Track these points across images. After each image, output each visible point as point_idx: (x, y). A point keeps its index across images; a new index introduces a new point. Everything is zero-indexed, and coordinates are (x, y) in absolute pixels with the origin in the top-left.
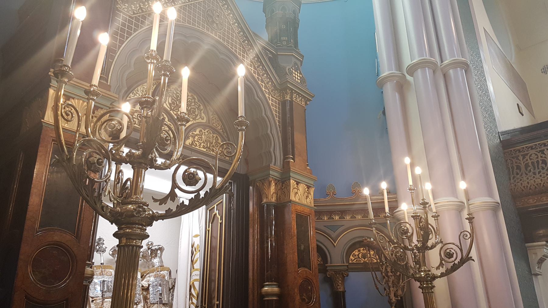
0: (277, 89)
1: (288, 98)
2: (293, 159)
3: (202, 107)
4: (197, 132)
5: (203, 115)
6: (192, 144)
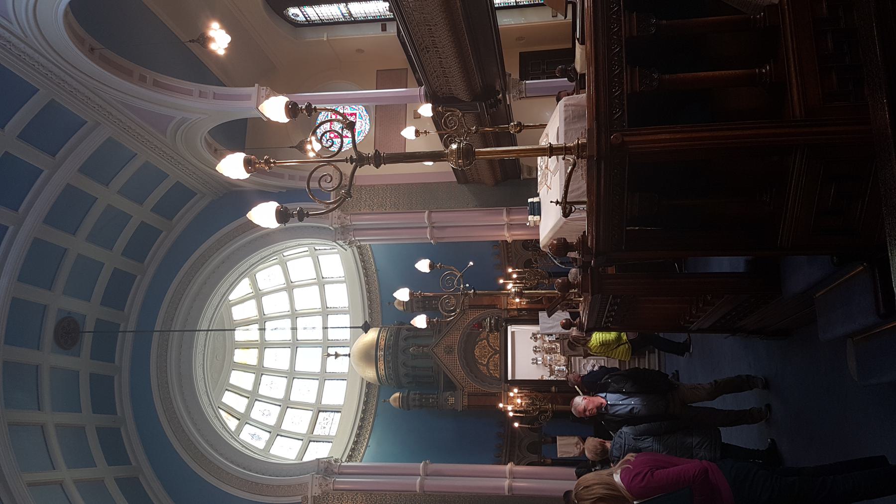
0: (464, 313)
1: (468, 307)
2: (497, 305)
3: (480, 343)
4: (492, 344)
5: (483, 342)
6: (498, 347)
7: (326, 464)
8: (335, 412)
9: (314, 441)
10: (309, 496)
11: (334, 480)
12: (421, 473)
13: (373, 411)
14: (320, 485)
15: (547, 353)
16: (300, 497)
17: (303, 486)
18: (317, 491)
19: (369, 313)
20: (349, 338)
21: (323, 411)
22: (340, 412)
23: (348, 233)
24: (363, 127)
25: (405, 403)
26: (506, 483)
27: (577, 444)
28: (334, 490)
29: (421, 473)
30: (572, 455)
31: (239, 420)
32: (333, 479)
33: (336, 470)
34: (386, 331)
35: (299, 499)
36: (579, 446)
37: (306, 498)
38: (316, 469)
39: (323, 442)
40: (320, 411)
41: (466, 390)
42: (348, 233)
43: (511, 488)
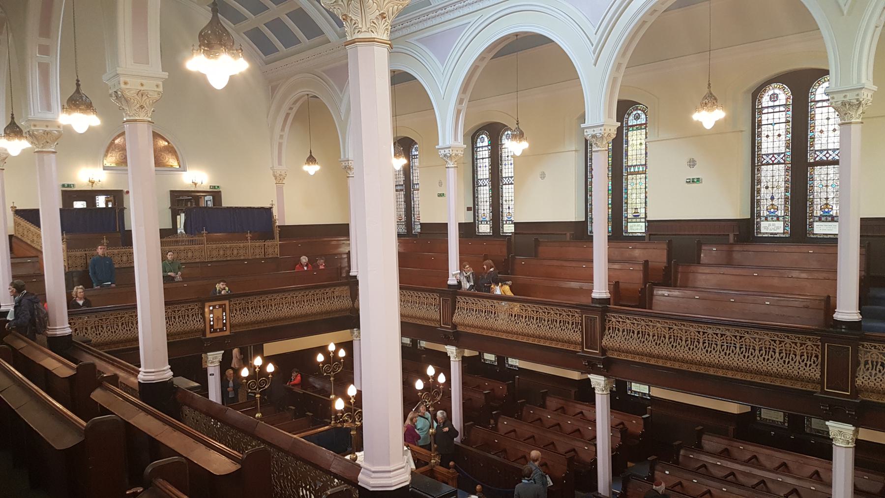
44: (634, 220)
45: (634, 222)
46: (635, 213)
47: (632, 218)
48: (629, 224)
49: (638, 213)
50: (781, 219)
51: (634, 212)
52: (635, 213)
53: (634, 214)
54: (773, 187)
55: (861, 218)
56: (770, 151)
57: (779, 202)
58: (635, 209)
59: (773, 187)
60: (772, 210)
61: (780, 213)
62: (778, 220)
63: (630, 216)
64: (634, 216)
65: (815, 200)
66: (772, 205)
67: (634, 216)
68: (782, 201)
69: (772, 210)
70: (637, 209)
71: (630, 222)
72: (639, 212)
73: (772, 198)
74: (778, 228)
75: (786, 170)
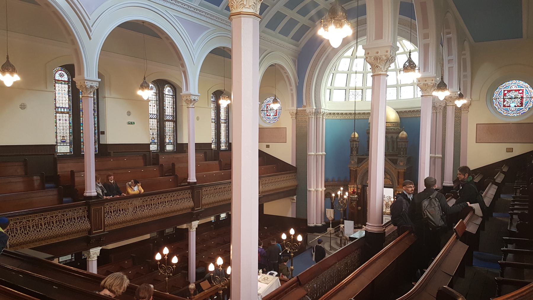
7: (320, 112)
8: (362, 97)
9: (346, 92)
10: (306, 108)
11: (313, 117)
12: (317, 153)
13: (360, 118)
14: (310, 112)
15: (387, 203)
16: (305, 104)
17: (310, 104)
18: (308, 111)
19: (410, 111)
20: (402, 98)
21: (362, 91)
22: (362, 100)
23: (434, 109)
24: (511, 112)
25: (353, 140)
26: (312, 189)
27: (331, 217)
28: (309, 118)
29: (317, 153)
30: (327, 215)
31: (352, 55)
32: (313, 117)
33: (318, 116)
34: (392, 126)
35: (305, 104)
36: (330, 218)
37: (305, 107)
38: (317, 108)
39: (345, 96)
40: (362, 90)
41: (358, 168)
42: (434, 109)
43: (310, 191)
44: (62, 144)
45: (65, 146)
46: (62, 139)
47: (60, 143)
48: (58, 147)
49: (65, 139)
50: (156, 143)
51: (62, 138)
52: (62, 139)
53: (62, 140)
54: (153, 129)
55: (196, 144)
56: (151, 113)
57: (155, 136)
58: (63, 137)
59: (153, 129)
60: (153, 140)
61: (156, 141)
62: (155, 144)
63: (59, 141)
64: (61, 141)
65: (166, 136)
66: (153, 137)
67: (61, 141)
68: (156, 136)
69: (153, 140)
70: (64, 137)
71: (59, 146)
72: (65, 138)
73: (153, 134)
74: (155, 148)
75: (157, 122)
